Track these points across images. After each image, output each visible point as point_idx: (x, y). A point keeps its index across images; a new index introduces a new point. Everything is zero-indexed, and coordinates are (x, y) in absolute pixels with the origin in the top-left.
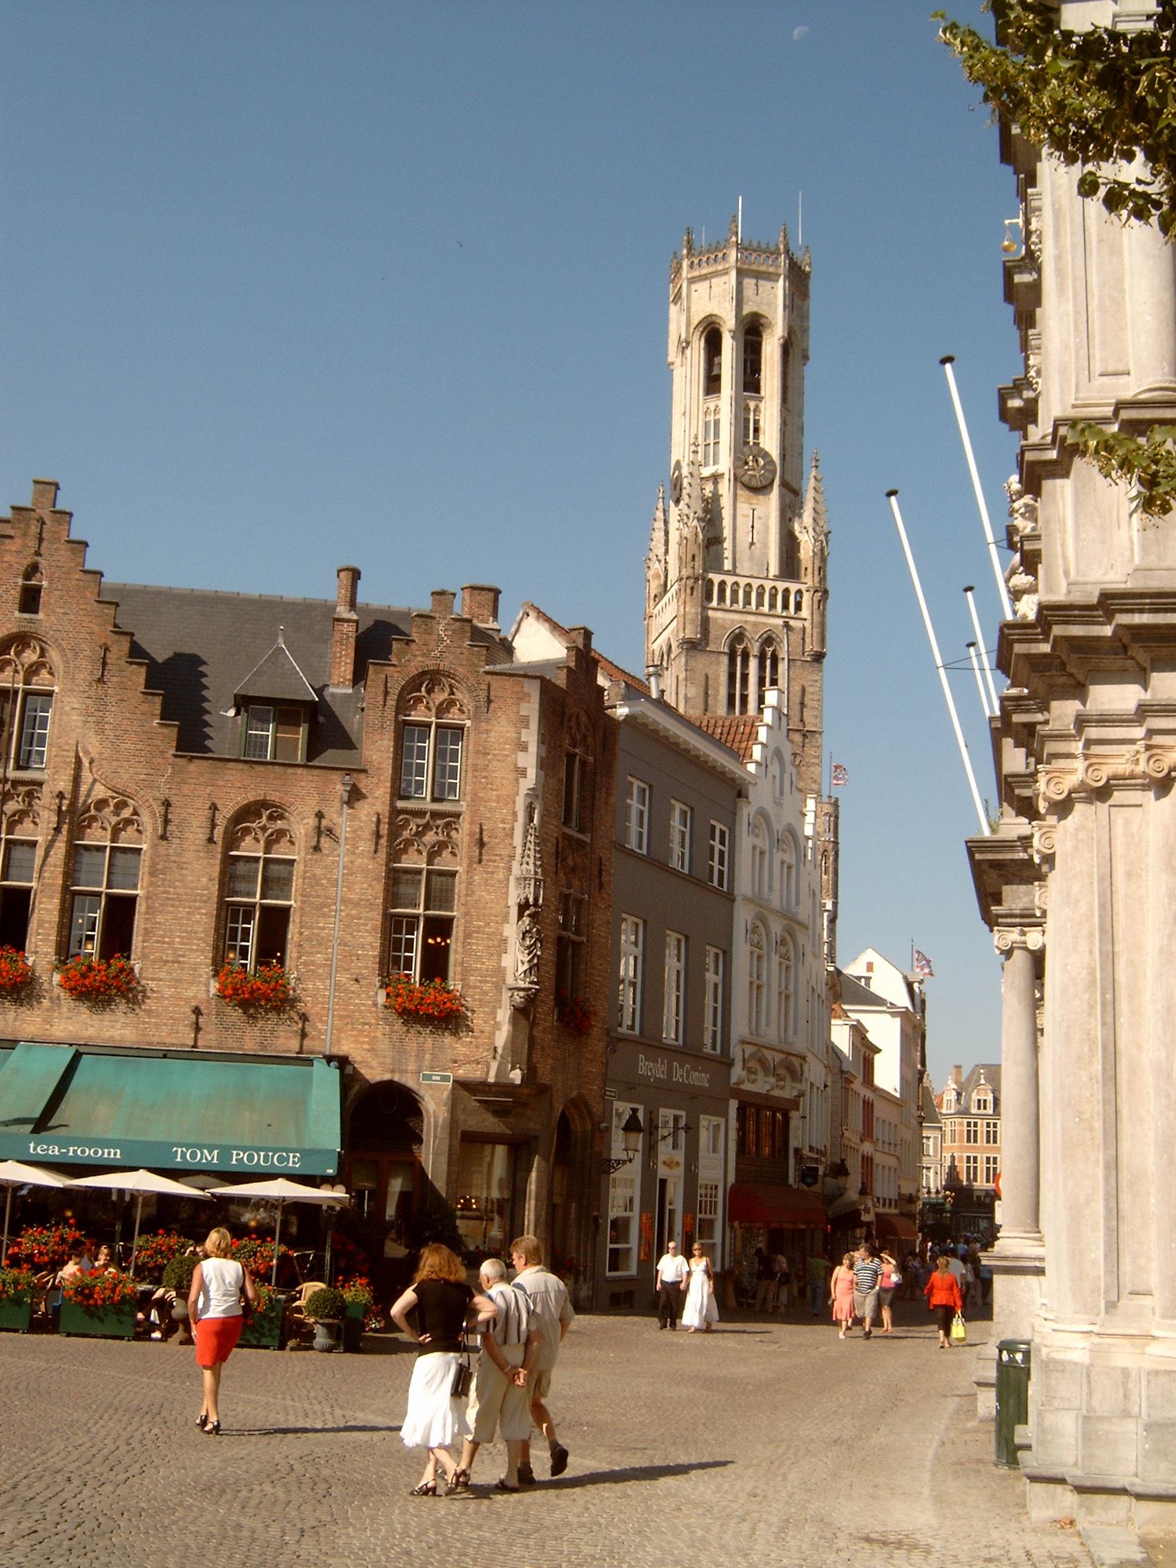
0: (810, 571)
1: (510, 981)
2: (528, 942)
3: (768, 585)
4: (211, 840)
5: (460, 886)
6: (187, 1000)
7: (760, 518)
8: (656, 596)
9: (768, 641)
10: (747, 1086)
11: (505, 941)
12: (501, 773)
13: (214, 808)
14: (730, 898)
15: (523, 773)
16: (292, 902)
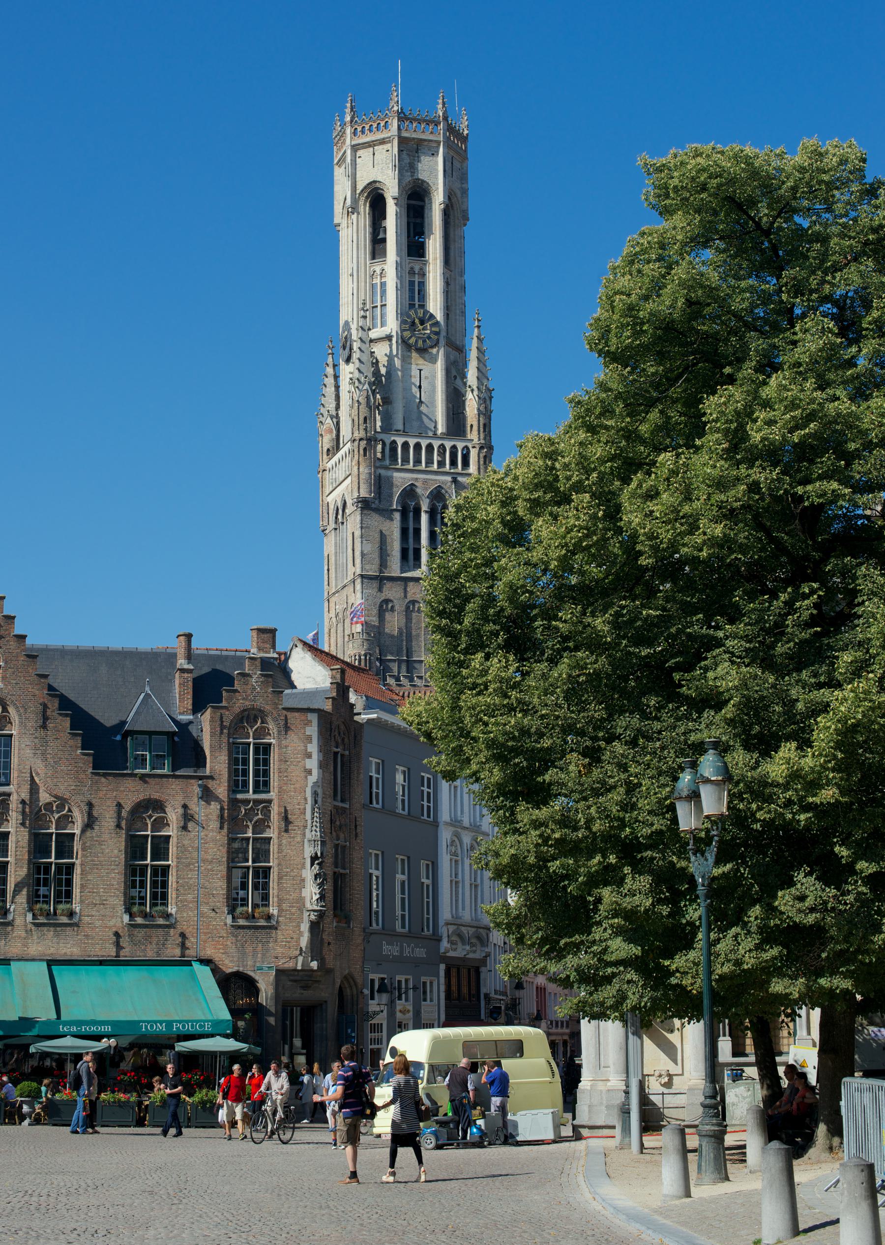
0: (475, 428)
1: (308, 906)
2: (318, 881)
3: (436, 444)
4: (118, 826)
5: (273, 848)
6: (110, 928)
7: (426, 378)
8: (328, 450)
9: (438, 496)
10: (451, 954)
11: (303, 880)
12: (296, 773)
13: (119, 805)
14: (435, 824)
15: (310, 772)
16: (170, 862)
